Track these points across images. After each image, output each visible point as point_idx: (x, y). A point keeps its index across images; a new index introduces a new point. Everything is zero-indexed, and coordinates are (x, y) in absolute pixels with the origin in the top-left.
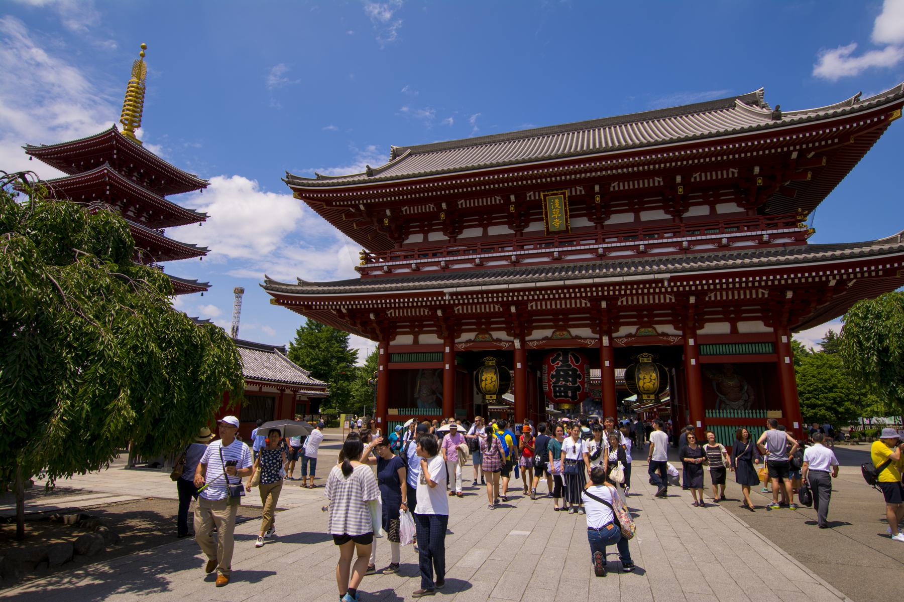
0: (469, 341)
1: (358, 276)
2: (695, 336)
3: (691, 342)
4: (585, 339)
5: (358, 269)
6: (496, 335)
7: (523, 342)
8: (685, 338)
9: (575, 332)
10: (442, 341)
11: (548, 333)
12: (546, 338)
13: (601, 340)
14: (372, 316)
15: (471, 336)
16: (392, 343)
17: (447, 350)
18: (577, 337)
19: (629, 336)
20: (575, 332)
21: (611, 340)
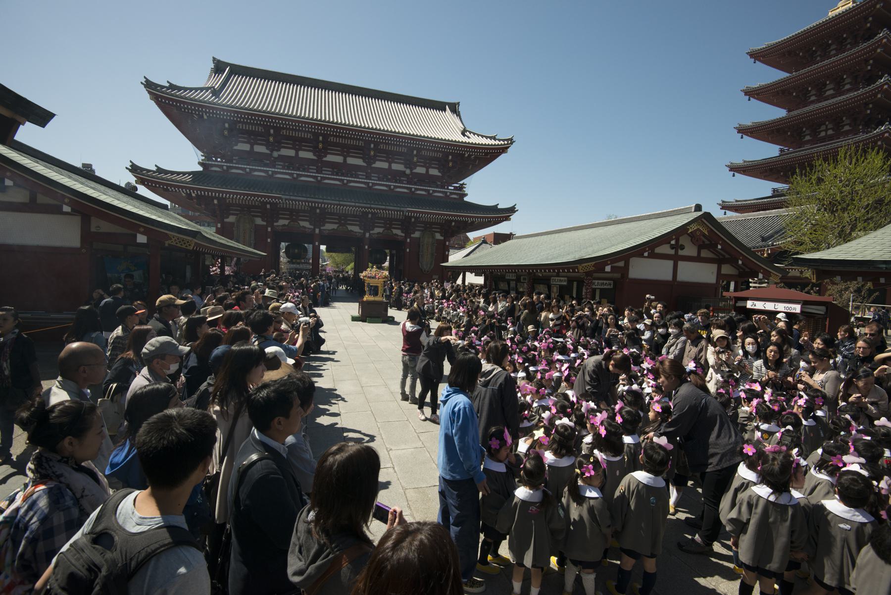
0: (284, 225)
1: (200, 169)
2: (410, 238)
3: (408, 240)
5: (200, 163)
6: (302, 224)
7: (320, 230)
8: (406, 238)
9: (350, 228)
10: (265, 223)
11: (335, 226)
14: (216, 202)
15: (286, 222)
16: (226, 220)
17: (269, 229)
19: (378, 233)
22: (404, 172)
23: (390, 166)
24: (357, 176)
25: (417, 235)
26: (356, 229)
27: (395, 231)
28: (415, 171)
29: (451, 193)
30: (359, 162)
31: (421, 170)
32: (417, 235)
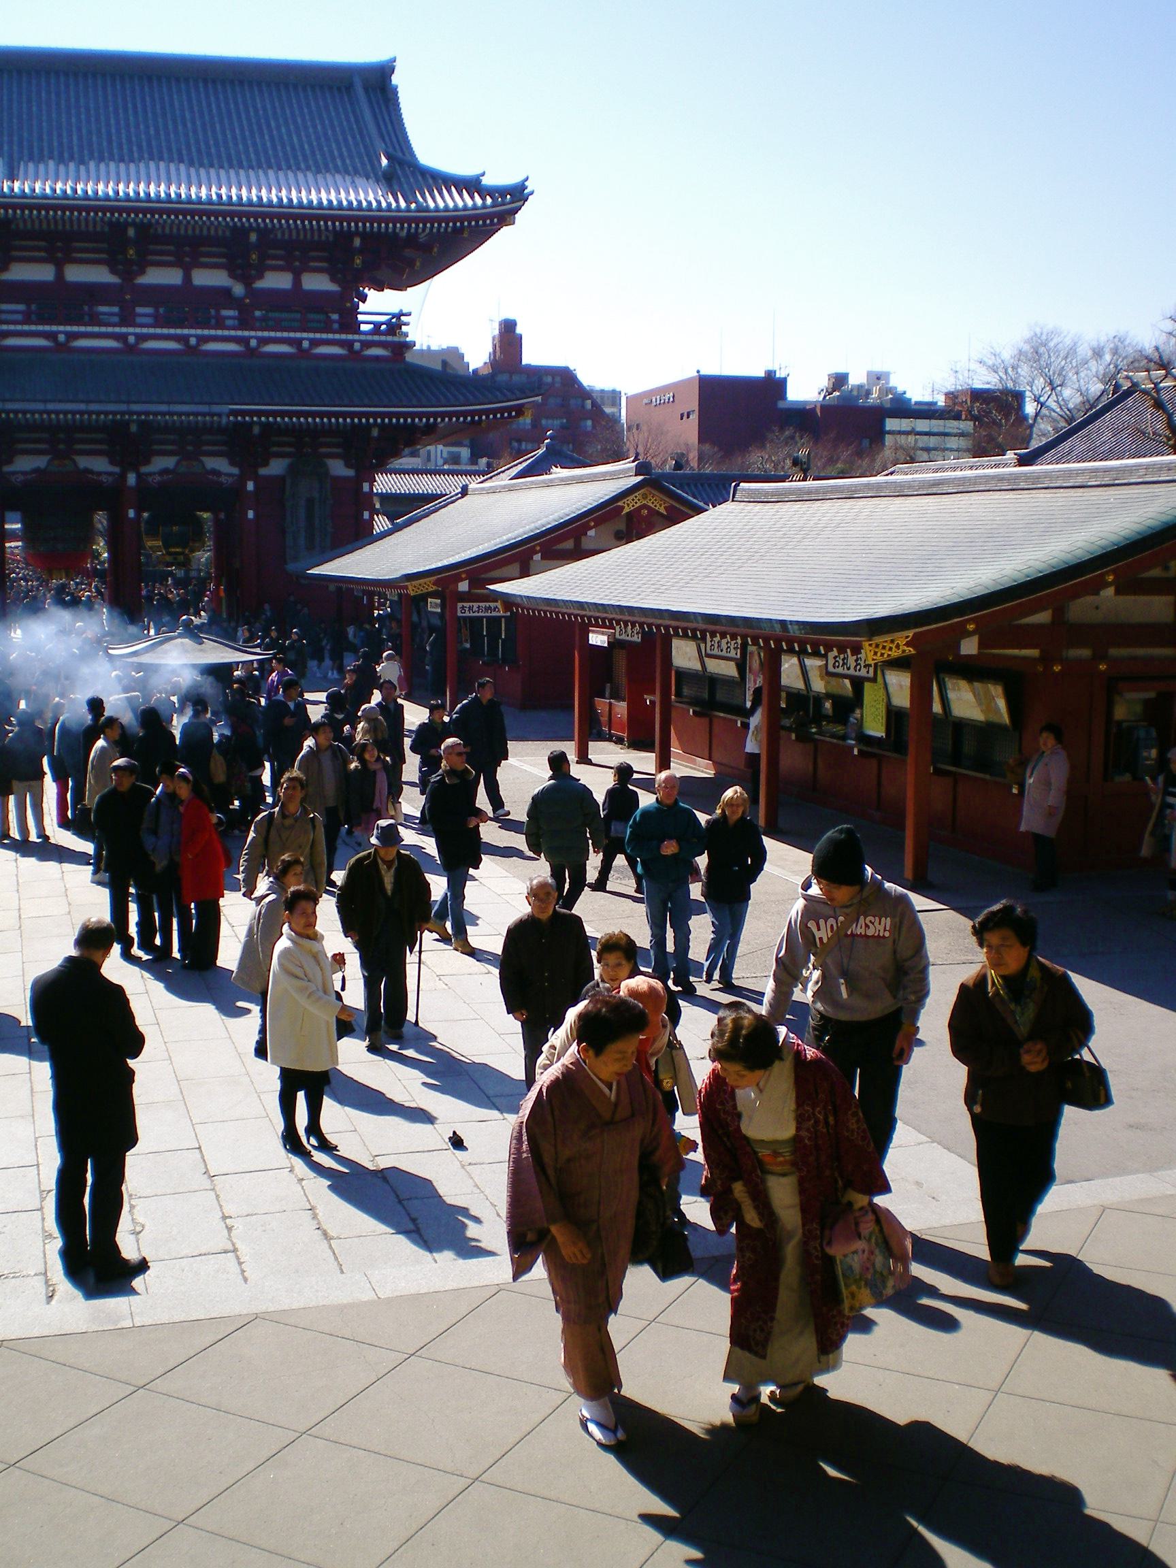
2: (257, 479)
3: (250, 486)
4: (100, 474)
9: (83, 462)
11: (41, 462)
12: (36, 470)
13: (123, 476)
18: (87, 471)
19: (165, 471)
20: (83, 462)
21: (139, 476)
22: (227, 292)
23: (187, 278)
24: (95, 320)
25: (276, 467)
26: (100, 464)
27: (212, 463)
28: (260, 284)
29: (367, 345)
30: (100, 275)
31: (277, 281)
32: (276, 467)
